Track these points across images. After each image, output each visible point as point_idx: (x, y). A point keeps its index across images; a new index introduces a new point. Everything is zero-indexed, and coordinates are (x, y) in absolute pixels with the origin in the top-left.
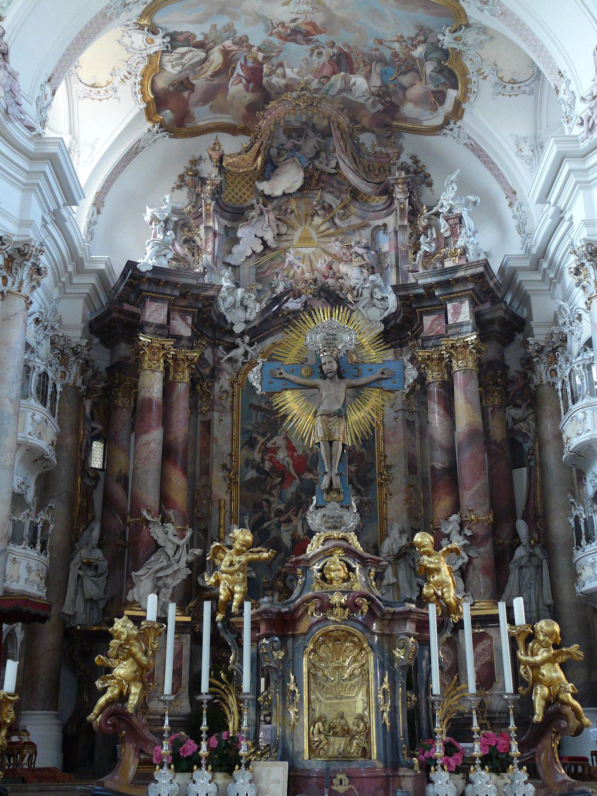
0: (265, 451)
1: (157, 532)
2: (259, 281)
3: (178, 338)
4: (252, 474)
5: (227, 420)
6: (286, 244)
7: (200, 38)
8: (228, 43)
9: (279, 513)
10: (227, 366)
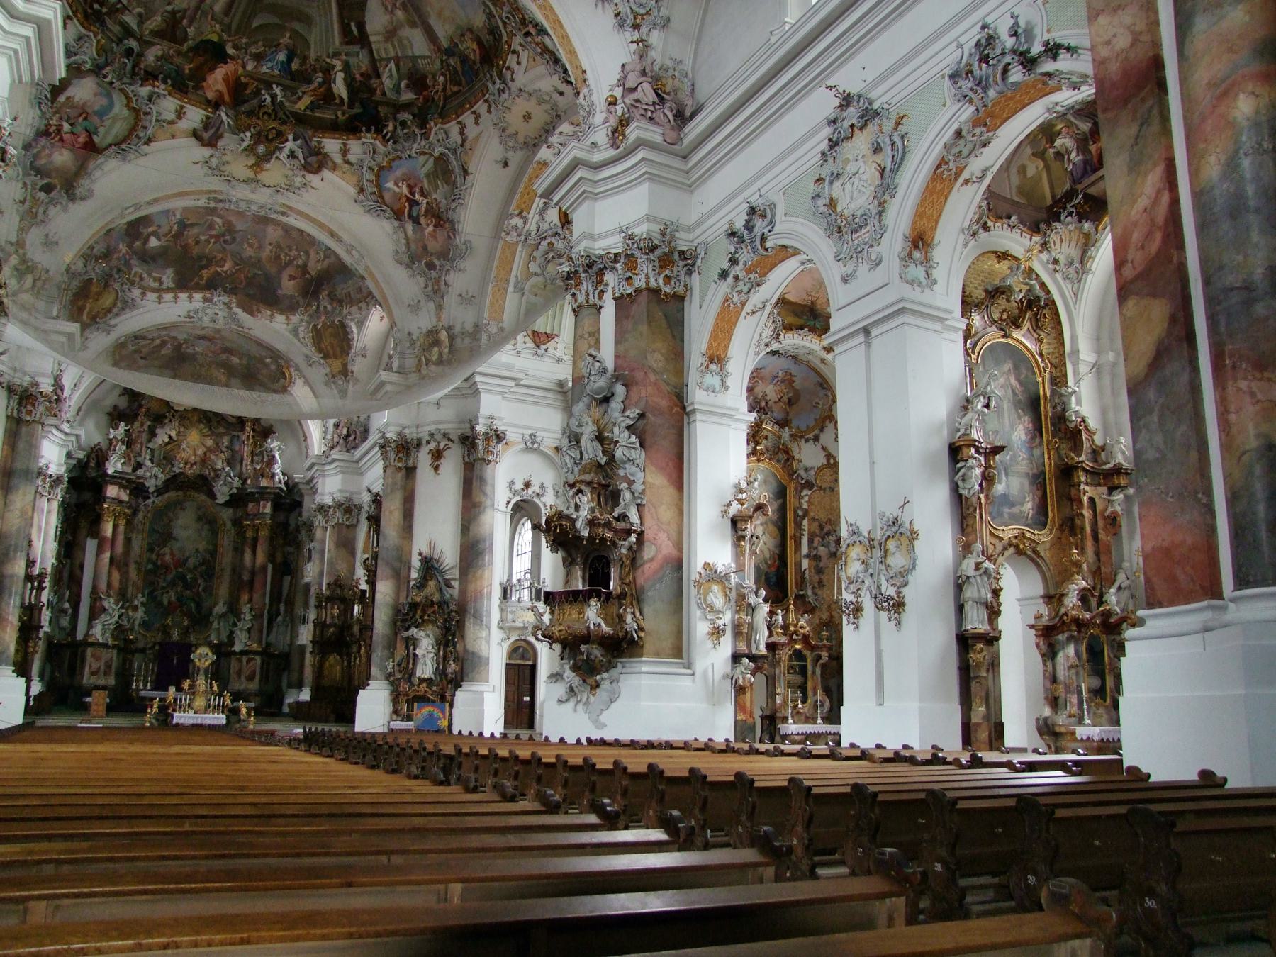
0: (158, 555)
1: (106, 604)
2: (164, 458)
3: (121, 502)
4: (150, 566)
5: (140, 537)
6: (181, 438)
7: (151, 337)
8: (166, 338)
9: (163, 588)
10: (143, 508)
